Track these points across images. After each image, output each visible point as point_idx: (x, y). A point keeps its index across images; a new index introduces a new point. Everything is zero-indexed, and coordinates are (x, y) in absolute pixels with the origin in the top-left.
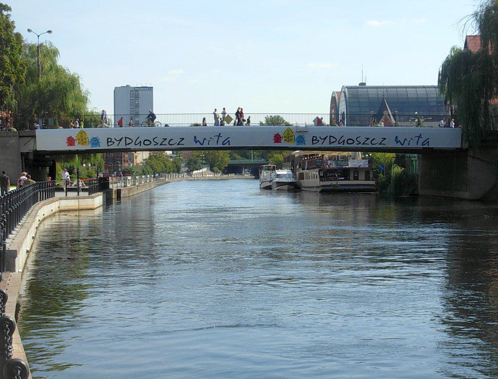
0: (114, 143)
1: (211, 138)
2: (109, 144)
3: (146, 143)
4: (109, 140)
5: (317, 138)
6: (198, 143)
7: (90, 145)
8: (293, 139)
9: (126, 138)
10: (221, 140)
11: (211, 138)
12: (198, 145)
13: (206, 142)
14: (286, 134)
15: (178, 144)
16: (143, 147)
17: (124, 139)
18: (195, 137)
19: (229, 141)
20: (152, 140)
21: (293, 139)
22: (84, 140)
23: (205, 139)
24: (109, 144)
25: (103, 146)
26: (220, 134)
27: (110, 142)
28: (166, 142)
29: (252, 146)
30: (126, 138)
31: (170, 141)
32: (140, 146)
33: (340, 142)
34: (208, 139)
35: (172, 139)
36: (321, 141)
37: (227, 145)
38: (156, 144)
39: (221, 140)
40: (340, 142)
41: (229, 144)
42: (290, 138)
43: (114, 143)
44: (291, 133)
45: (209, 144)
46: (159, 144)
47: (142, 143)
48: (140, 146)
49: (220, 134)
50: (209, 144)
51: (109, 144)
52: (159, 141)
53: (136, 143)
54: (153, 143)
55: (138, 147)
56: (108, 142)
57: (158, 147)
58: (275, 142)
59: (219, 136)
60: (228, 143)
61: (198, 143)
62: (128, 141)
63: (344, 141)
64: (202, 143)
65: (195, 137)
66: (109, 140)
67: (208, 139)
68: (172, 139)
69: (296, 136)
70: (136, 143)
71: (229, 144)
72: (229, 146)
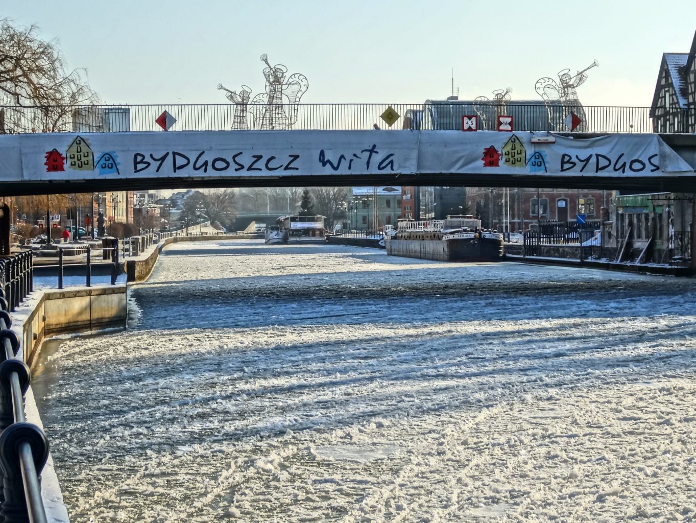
0: (149, 164)
1: (355, 155)
2: (138, 169)
3: (220, 165)
4: (139, 159)
5: (571, 158)
6: (328, 164)
7: (97, 170)
8: (523, 159)
9: (174, 154)
10: (377, 158)
11: (355, 155)
12: (328, 171)
13: (344, 164)
14: (509, 148)
15: (286, 168)
16: (212, 174)
17: (170, 157)
18: (322, 154)
19: (392, 162)
20: (230, 160)
21: (523, 159)
22: (83, 159)
23: (342, 157)
24: (138, 169)
25: (127, 172)
26: (374, 146)
27: (141, 162)
28: (261, 164)
29: (438, 172)
30: (174, 154)
31: (269, 161)
32: (205, 171)
33: (617, 167)
34: (349, 156)
35: (273, 158)
36: (580, 165)
37: (387, 171)
38: (238, 167)
39: (377, 158)
40: (617, 168)
41: (392, 169)
42: (517, 156)
43: (149, 164)
44: (518, 148)
45: (350, 168)
46: (246, 167)
47: (210, 164)
48: (205, 171)
49: (374, 146)
50: (350, 168)
51: (140, 166)
52: (246, 160)
53: (197, 166)
54: (233, 166)
55: (200, 174)
56: (136, 163)
57: (244, 173)
58: (485, 165)
59: (372, 151)
60: (390, 165)
61: (328, 164)
62: (180, 161)
63: (624, 165)
64: (336, 165)
65: (322, 154)
66: (139, 159)
67: (349, 156)
68: (273, 158)
69: (530, 151)
70: (197, 166)
71: (392, 169)
72: (393, 172)
